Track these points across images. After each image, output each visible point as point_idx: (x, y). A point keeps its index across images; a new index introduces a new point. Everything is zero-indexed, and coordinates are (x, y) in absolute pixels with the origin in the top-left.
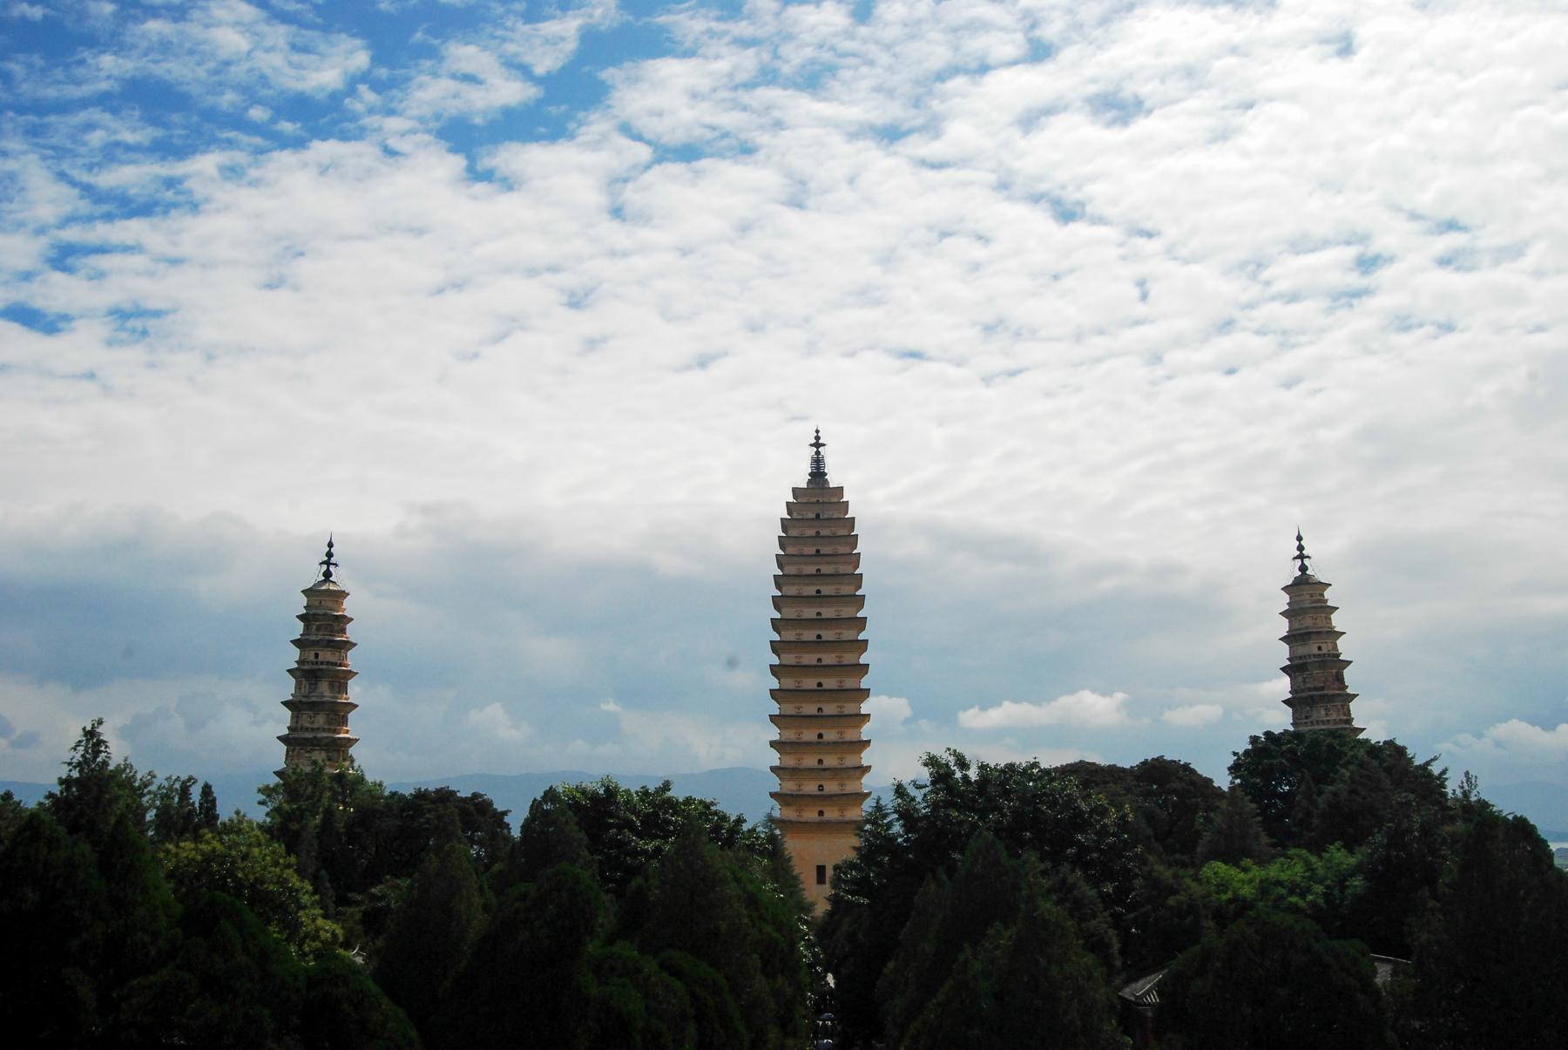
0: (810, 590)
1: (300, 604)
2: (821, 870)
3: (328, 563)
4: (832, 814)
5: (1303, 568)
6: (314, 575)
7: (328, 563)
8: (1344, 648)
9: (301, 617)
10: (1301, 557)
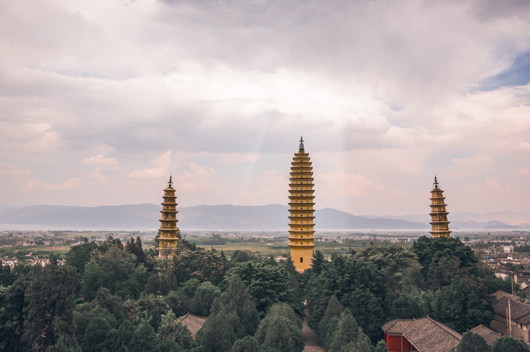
1: (163, 194)
2: (302, 259)
4: (305, 244)
5: (436, 187)
6: (166, 186)
8: (447, 209)
9: (163, 197)
10: (436, 183)
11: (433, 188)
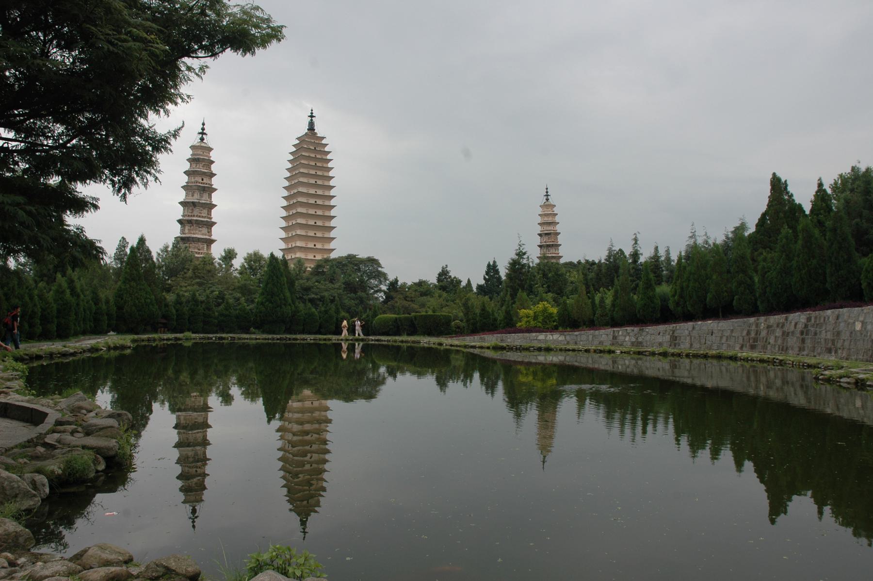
0: (312, 181)
3: (203, 133)
5: (547, 200)
7: (203, 133)
10: (547, 195)
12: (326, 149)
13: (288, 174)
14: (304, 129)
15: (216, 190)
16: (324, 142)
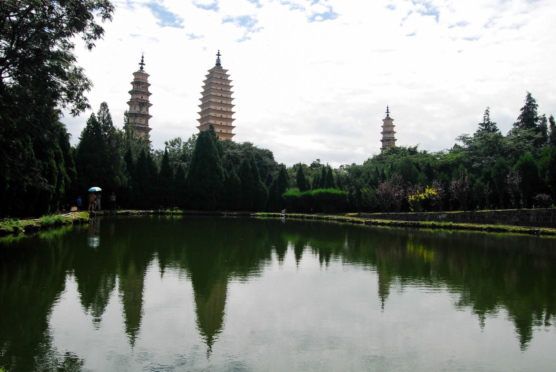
0: (219, 101)
5: (388, 115)
10: (388, 112)
11: (385, 116)
12: (229, 78)
13: (202, 96)
14: (213, 65)
15: (152, 105)
16: (227, 73)
